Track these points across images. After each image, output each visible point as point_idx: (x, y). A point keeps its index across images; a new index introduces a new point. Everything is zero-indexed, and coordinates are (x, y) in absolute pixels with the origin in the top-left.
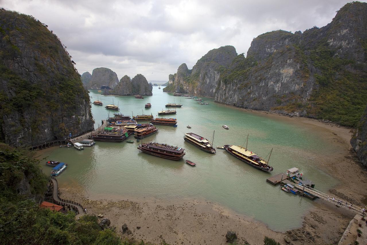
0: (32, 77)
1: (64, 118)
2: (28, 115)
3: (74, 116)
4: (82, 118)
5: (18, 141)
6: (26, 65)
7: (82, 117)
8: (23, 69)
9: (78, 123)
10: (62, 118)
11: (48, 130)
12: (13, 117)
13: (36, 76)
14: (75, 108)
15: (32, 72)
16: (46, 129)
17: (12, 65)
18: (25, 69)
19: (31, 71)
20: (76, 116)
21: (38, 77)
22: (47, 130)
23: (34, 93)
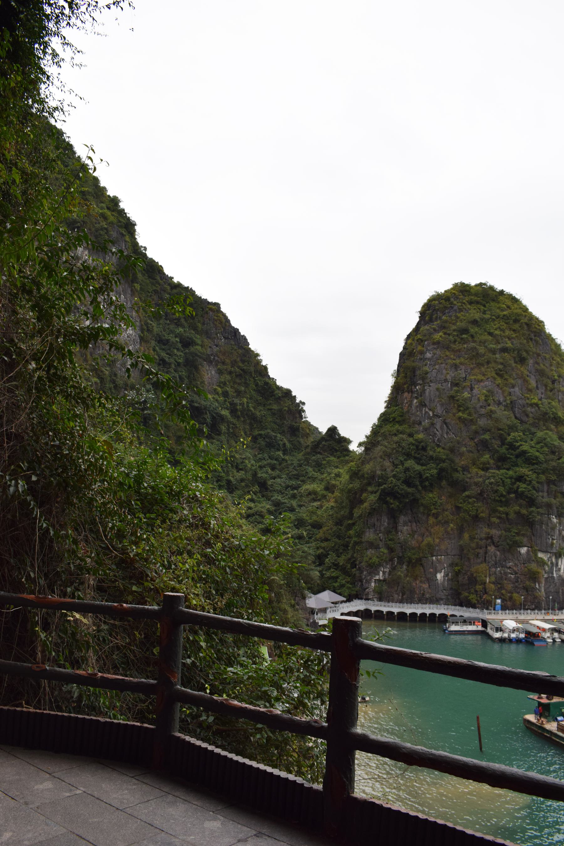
0: (437, 430)
1: (489, 548)
2: (407, 526)
3: (524, 550)
4: (552, 563)
5: (373, 584)
6: (431, 400)
7: (554, 560)
8: (424, 412)
9: (534, 577)
10: (486, 547)
11: (446, 575)
12: (376, 523)
13: (447, 427)
14: (529, 522)
15: (440, 417)
16: (441, 572)
17: (407, 405)
18: (427, 410)
19: (437, 416)
20: (528, 551)
21: (450, 430)
22: (442, 574)
23: (432, 471)
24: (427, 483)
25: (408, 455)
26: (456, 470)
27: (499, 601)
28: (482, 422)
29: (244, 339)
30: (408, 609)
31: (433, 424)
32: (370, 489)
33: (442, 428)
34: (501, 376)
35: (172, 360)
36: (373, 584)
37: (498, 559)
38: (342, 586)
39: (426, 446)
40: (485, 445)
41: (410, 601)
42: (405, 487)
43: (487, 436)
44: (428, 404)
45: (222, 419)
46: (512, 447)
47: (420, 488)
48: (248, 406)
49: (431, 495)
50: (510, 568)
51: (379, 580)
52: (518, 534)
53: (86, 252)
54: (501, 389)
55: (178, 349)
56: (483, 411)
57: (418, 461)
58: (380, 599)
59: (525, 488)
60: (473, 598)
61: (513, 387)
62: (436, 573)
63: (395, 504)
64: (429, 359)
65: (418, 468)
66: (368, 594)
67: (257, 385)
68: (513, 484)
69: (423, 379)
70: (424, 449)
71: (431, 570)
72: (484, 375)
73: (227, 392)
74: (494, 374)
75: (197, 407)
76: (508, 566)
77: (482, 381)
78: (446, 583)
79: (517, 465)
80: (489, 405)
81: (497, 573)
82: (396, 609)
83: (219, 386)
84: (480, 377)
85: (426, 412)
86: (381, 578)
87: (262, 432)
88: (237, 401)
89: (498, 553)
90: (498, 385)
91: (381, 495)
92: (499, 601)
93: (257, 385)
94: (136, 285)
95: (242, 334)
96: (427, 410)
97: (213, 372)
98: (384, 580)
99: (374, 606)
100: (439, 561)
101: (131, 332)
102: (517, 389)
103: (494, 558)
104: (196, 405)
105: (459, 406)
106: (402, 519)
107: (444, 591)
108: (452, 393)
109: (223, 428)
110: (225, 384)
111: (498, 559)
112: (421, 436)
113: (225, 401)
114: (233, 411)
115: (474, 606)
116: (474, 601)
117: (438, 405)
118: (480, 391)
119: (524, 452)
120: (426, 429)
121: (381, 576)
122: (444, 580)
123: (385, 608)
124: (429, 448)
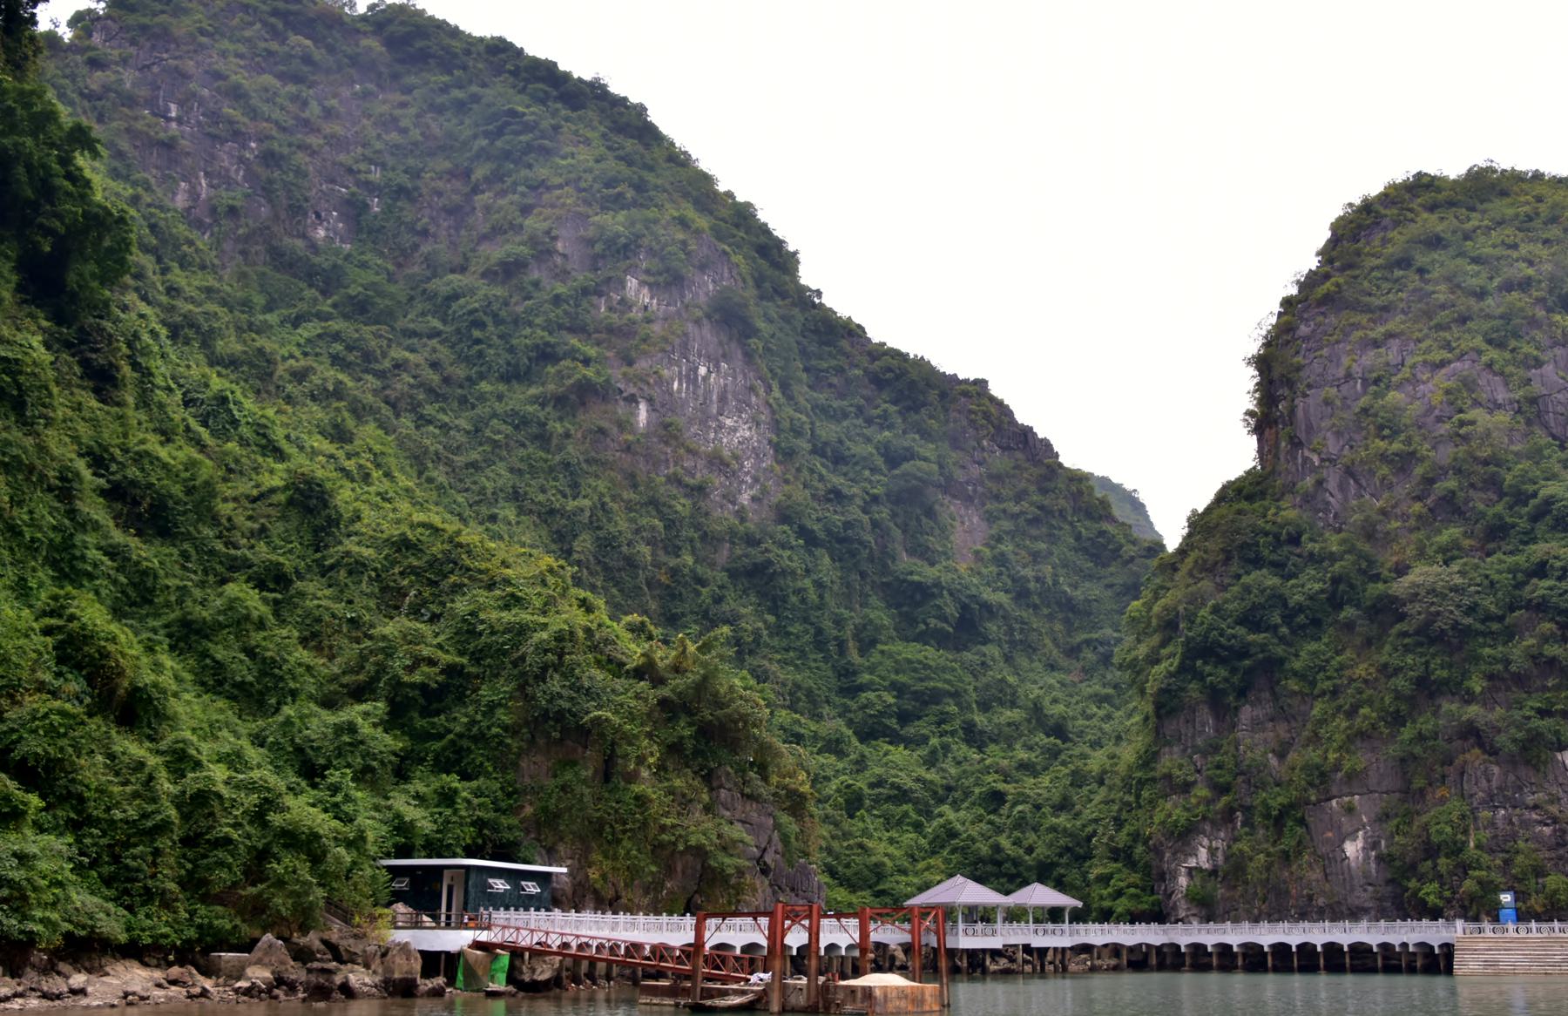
5: (1183, 881)
13: (1356, 481)
18: (1307, 453)
22: (1360, 843)
24: (1301, 619)
25: (1257, 562)
26: (1376, 578)
27: (1506, 898)
28: (1446, 454)
29: (1047, 445)
30: (1267, 936)
31: (1320, 483)
32: (1164, 652)
33: (1342, 488)
34: (1501, 345)
35: (855, 490)
36: (1183, 881)
37: (1494, 784)
38: (1119, 894)
39: (1300, 535)
40: (1451, 507)
41: (1276, 914)
42: (1240, 631)
43: (1451, 483)
44: (1303, 436)
45: (987, 607)
46: (1521, 498)
47: (1284, 630)
48: (1056, 583)
49: (1313, 646)
50: (1536, 807)
51: (1199, 869)
52: (1543, 713)
53: (645, 291)
54: (1502, 374)
55: (874, 470)
56: (1444, 429)
57: (1278, 567)
58: (1208, 919)
59: (1551, 589)
60: (1430, 892)
61: (1539, 364)
62: (1343, 842)
63: (1218, 674)
64: (1306, 339)
65: (1273, 581)
66: (1175, 908)
67: (1078, 538)
68: (1519, 586)
69: (1290, 384)
70: (1295, 540)
71: (1330, 834)
72: (1451, 350)
73: (1002, 554)
74: (1478, 341)
75: (919, 584)
76: (1531, 804)
77: (1443, 364)
78: (1373, 866)
79: (1534, 540)
80: (1461, 411)
81: (1500, 824)
82: (1235, 935)
83: (987, 545)
84: (1438, 356)
85: (1306, 460)
86: (1206, 866)
87: (1095, 636)
88: (1028, 572)
89: (1496, 769)
90: (1489, 366)
91: (1184, 657)
92: (1506, 898)
93: (1078, 538)
94: (753, 341)
95: (1040, 436)
96: (1307, 453)
97: (975, 519)
98: (1214, 872)
99: (1184, 935)
100: (1350, 810)
101: (747, 434)
102: (1549, 369)
103: (1484, 783)
104: (916, 578)
105: (1381, 427)
106: (1247, 713)
107: (1370, 888)
108: (1364, 401)
109: (992, 628)
110: (999, 540)
111: (1494, 784)
112: (1291, 514)
113: (1000, 574)
114: (1021, 595)
115: (1435, 914)
116: (1432, 899)
117: (1329, 434)
118: (1435, 387)
119: (1549, 501)
120: (1308, 499)
121: (1202, 858)
122: (1367, 858)
123: (1211, 936)
124: (1304, 538)
